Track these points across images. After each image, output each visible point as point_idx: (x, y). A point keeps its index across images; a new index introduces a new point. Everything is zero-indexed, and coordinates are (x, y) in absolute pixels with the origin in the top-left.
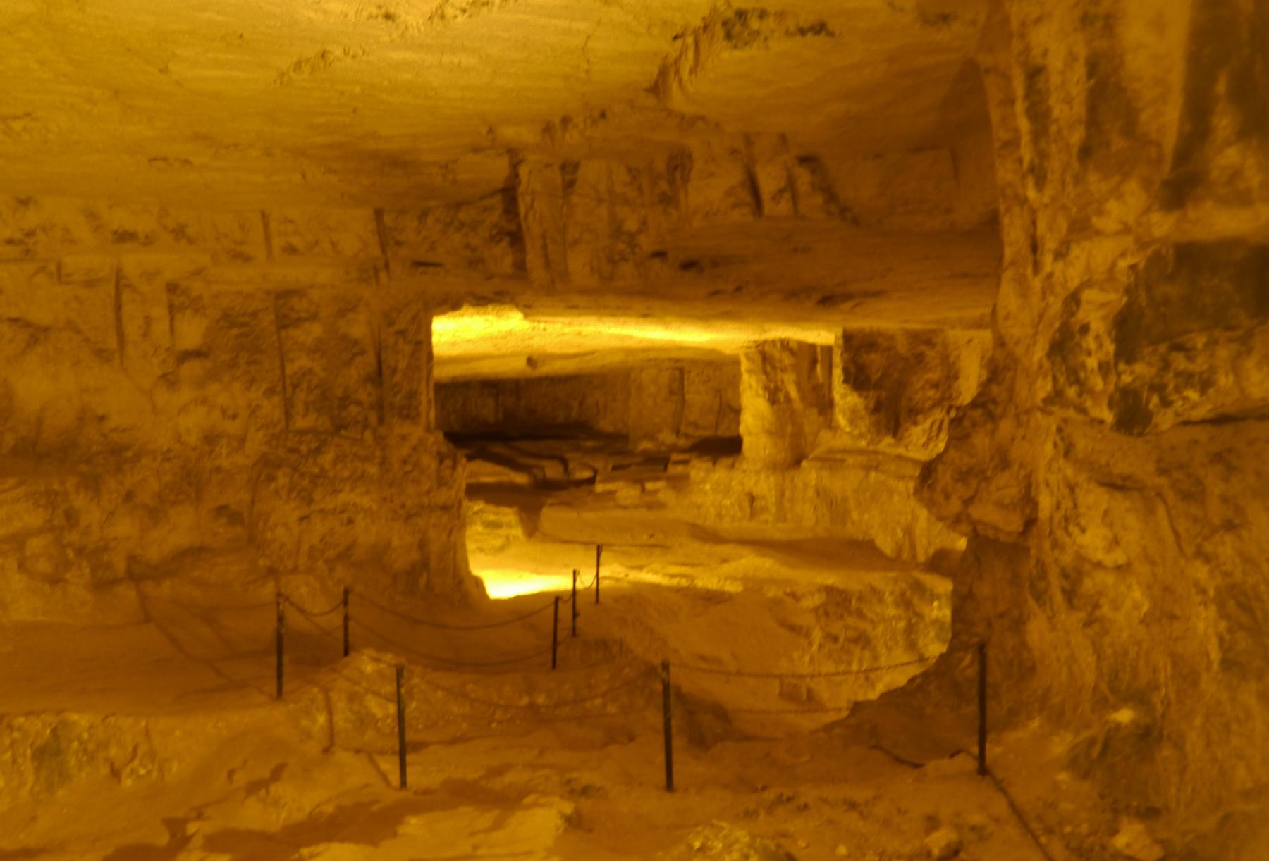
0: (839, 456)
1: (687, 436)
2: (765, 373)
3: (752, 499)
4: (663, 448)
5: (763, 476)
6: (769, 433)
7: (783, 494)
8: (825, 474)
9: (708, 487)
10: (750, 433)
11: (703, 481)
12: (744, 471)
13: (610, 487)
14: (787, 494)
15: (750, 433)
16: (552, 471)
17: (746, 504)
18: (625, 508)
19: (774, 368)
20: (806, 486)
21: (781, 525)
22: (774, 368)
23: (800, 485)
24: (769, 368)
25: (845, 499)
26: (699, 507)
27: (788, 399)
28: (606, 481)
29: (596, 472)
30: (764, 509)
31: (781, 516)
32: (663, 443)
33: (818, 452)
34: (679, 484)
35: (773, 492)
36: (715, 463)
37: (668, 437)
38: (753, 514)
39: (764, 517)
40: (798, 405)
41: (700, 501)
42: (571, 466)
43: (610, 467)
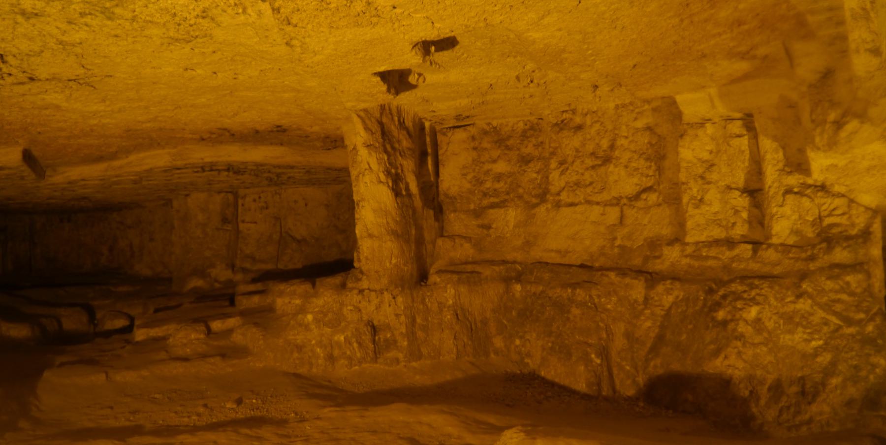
0: (469, 268)
1: (244, 270)
2: (386, 151)
3: (374, 330)
4: (217, 285)
5: (387, 296)
6: (394, 233)
7: (414, 320)
8: (463, 289)
9: (310, 317)
10: (371, 236)
11: (302, 310)
12: (361, 291)
13: (155, 332)
14: (419, 320)
15: (371, 236)
16: (72, 321)
17: (367, 338)
18: (185, 359)
19: (393, 148)
20: (441, 306)
21: (414, 364)
22: (393, 148)
23: (435, 307)
24: (388, 147)
25: (485, 322)
26: (299, 348)
27: (409, 195)
28: (146, 326)
29: (132, 319)
30: (391, 344)
31: (415, 354)
32: (216, 281)
33: (439, 264)
34: (263, 318)
35: (403, 318)
36: (314, 285)
37: (221, 273)
38: (377, 354)
39: (391, 354)
40: (418, 202)
41: (300, 339)
42: (99, 315)
43: (152, 310)
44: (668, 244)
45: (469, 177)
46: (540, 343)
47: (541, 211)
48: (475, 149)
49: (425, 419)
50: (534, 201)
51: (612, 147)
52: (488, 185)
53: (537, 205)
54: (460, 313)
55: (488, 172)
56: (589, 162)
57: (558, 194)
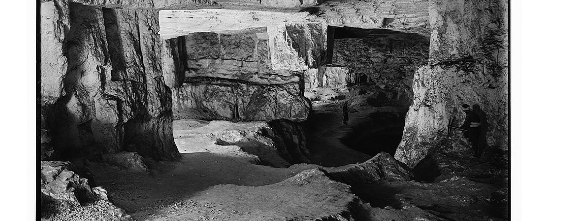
6: (173, 71)
8: (194, 87)
44: (255, 74)
45: (194, 48)
46: (217, 103)
47: (218, 61)
48: (196, 39)
49: (190, 122)
50: (216, 57)
51: (240, 42)
52: (200, 51)
53: (216, 59)
54: (194, 96)
55: (200, 46)
56: (234, 46)
57: (223, 56)
